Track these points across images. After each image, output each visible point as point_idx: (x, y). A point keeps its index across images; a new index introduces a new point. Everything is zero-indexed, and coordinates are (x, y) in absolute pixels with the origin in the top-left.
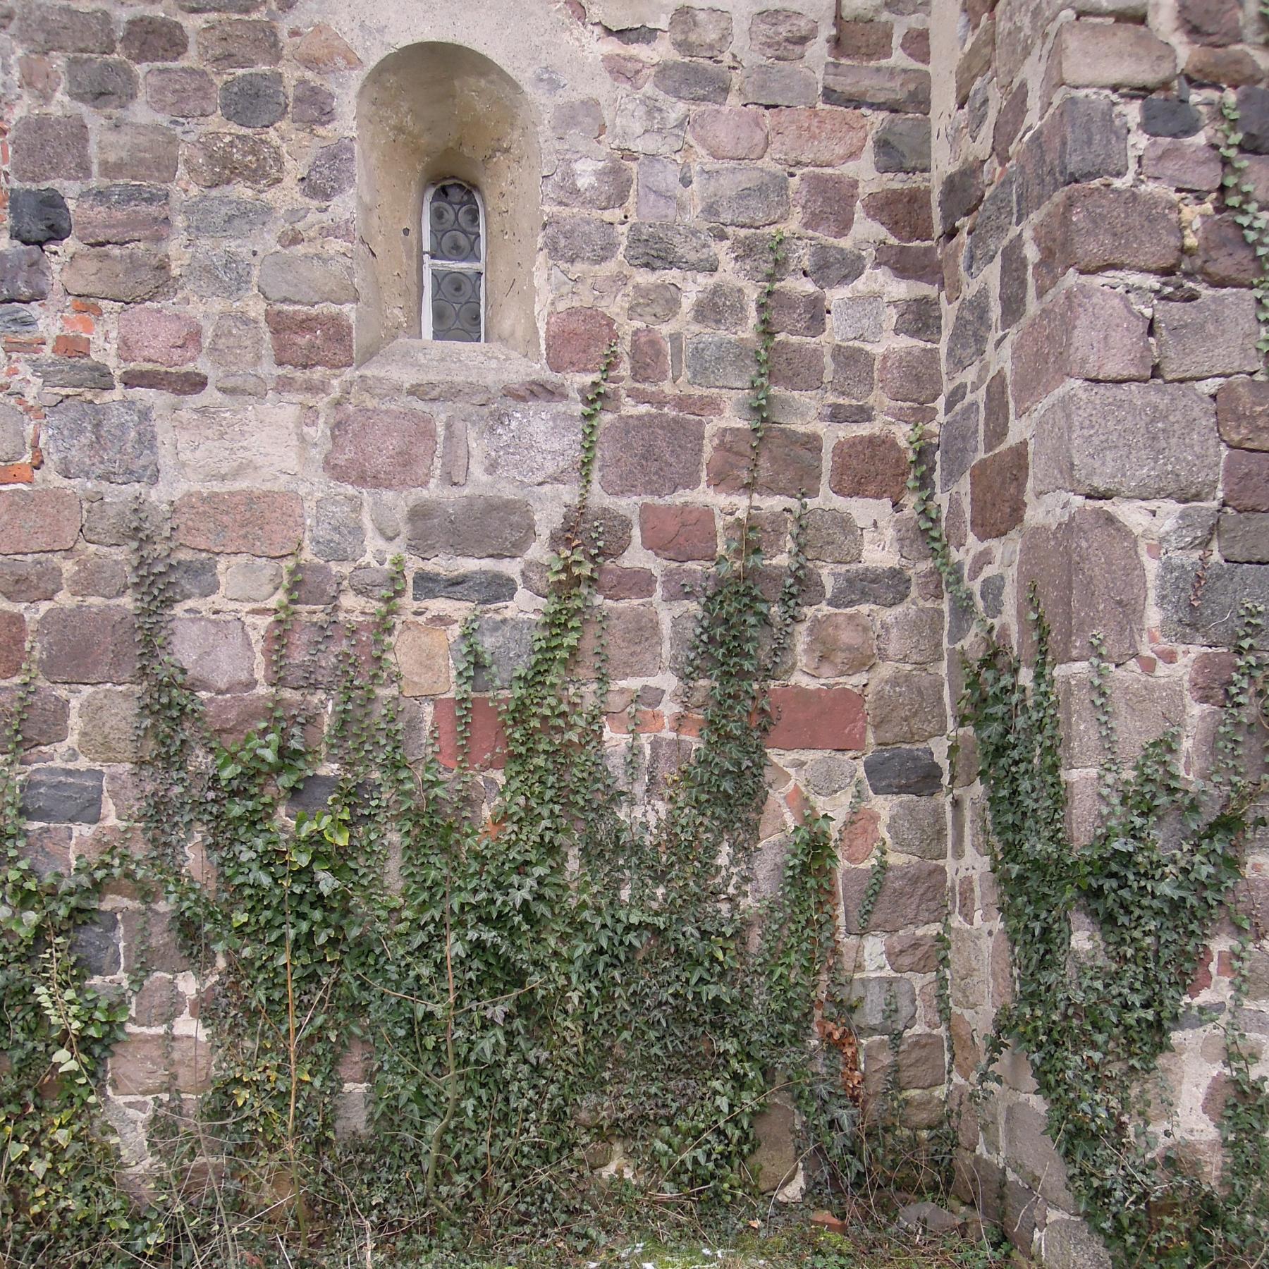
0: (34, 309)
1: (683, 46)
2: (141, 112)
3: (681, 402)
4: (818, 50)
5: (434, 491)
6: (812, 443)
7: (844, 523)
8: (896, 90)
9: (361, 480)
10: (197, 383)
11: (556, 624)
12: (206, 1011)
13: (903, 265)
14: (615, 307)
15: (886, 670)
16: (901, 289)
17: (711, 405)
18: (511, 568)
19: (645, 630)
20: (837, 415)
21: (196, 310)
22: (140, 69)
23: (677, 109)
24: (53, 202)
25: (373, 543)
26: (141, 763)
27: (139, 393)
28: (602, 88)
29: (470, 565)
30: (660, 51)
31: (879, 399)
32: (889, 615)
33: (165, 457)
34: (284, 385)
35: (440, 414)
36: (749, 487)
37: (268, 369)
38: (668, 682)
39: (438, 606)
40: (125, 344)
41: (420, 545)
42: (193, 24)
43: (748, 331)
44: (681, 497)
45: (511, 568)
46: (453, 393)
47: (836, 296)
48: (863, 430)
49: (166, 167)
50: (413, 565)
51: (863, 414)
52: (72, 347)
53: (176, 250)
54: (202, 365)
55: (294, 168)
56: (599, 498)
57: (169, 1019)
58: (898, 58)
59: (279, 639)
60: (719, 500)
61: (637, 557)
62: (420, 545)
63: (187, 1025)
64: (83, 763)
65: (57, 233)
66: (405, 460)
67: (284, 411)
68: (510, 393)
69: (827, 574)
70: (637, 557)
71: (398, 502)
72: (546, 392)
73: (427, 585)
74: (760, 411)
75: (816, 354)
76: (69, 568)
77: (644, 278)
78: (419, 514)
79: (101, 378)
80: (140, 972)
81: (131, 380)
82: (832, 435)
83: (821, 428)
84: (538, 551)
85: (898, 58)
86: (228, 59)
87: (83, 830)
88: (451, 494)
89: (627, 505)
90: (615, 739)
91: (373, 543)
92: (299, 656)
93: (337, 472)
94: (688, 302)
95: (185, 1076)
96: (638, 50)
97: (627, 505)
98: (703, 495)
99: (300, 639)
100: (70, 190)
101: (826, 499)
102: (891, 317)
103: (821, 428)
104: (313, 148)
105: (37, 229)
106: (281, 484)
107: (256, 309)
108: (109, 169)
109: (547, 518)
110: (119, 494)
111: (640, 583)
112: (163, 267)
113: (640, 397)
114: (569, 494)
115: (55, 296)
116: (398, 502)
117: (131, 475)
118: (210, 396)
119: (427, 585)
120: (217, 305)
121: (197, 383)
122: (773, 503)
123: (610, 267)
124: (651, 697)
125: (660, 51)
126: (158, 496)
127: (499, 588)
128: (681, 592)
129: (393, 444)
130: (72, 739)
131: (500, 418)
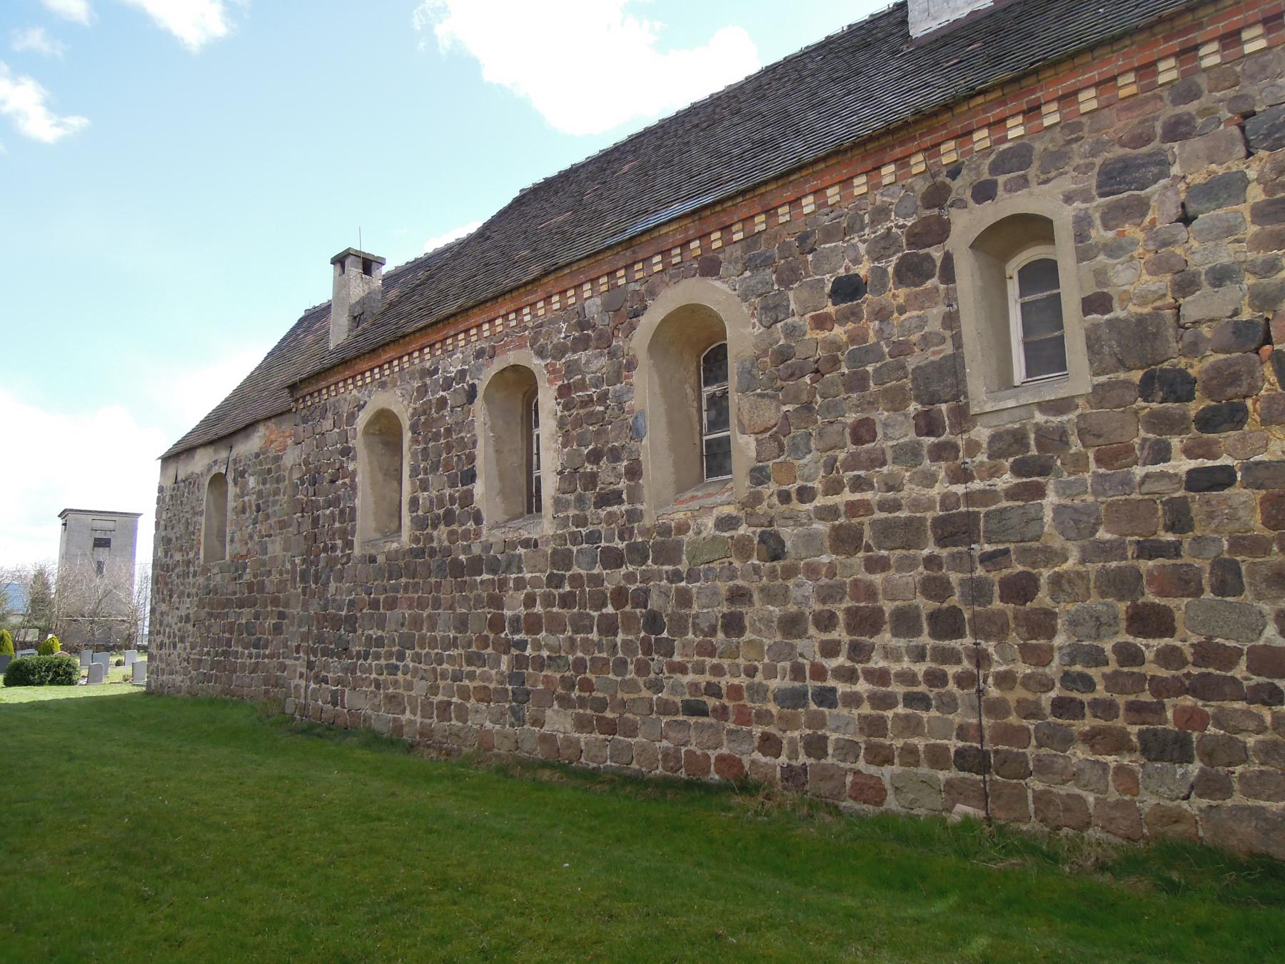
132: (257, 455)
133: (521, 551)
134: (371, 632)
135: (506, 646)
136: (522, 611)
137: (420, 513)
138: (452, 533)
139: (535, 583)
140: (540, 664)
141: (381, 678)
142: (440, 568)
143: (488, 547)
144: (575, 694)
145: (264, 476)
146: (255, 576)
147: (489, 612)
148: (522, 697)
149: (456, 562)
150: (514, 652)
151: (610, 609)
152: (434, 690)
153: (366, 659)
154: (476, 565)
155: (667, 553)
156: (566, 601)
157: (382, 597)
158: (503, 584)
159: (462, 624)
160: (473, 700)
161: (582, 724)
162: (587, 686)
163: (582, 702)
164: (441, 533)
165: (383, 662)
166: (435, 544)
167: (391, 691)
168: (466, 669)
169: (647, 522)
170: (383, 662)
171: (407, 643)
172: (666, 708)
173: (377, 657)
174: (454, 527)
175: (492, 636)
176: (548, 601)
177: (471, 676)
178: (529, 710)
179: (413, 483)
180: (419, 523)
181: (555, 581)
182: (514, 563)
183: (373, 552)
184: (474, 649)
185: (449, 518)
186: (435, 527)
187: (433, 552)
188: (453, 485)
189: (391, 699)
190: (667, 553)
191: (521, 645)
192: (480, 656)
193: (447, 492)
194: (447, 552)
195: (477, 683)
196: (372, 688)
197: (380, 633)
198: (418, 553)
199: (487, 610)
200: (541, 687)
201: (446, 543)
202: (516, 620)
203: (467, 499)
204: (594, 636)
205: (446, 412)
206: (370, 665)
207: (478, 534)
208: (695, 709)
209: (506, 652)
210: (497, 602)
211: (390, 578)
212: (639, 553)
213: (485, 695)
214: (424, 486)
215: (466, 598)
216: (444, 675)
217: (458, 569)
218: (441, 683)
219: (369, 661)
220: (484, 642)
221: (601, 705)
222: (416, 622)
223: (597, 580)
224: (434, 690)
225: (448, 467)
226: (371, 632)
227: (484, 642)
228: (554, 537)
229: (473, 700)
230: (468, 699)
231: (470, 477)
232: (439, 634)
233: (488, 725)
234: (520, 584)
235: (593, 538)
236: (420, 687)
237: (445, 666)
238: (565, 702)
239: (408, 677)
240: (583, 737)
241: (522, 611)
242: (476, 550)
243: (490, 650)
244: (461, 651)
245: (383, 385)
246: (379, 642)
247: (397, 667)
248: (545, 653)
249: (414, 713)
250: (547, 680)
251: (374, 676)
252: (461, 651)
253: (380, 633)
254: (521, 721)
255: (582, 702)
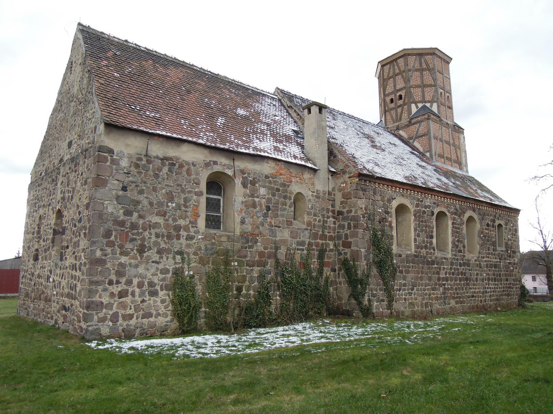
0: (267, 218)
1: (317, 193)
2: (276, 198)
3: (317, 231)
4: (327, 194)
5: (298, 239)
6: (327, 235)
7: (329, 244)
8: (332, 199)
9: (293, 238)
10: (280, 227)
11: (308, 254)
12: (280, 296)
13: (334, 217)
14: (312, 220)
15: (332, 259)
16: (333, 220)
17: (319, 231)
18: (304, 248)
19: (314, 254)
20: (328, 233)
21: (280, 219)
22: (277, 193)
23: (317, 200)
24: (269, 207)
25: (294, 245)
26: (275, 268)
27: (276, 228)
28: (311, 198)
29: (301, 247)
30: (315, 194)
31: (331, 231)
32: (332, 253)
33: (277, 235)
34: (287, 228)
35: (299, 231)
36: (322, 240)
37: (286, 226)
38: (316, 260)
39: (299, 252)
40: (275, 223)
41: (297, 245)
42: (281, 188)
43: (322, 223)
44: (317, 241)
45: (304, 248)
46: (300, 229)
47: (328, 220)
48: (330, 234)
49: (278, 204)
50: (297, 247)
51: (330, 233)
52: (270, 222)
53: (279, 213)
54: (281, 225)
55: (288, 205)
56: (311, 241)
57: (276, 297)
58: (333, 196)
59: (286, 255)
60: (320, 241)
61: (314, 247)
62: (297, 245)
63: (278, 298)
64: (270, 268)
65: (270, 210)
66: (296, 236)
67: (287, 230)
68: (304, 229)
69: (328, 249)
70: (314, 247)
71: (295, 240)
72: (307, 229)
73: (298, 249)
74: (323, 232)
75: (327, 226)
76: (269, 246)
77: (314, 218)
78: (297, 242)
79: (272, 226)
80: (274, 292)
81: (275, 226)
82: (328, 234)
83: (327, 234)
84: (306, 246)
85: (333, 196)
86: (283, 193)
87: (270, 276)
88: (300, 240)
89: (313, 241)
90: (312, 266)
91: (294, 245)
92: (288, 257)
93: (291, 237)
94: (317, 220)
95: (278, 303)
96: (313, 194)
97: (313, 241)
98: (319, 241)
99: (288, 255)
100: (271, 205)
101: (328, 241)
102: (332, 223)
103: (327, 234)
104: (290, 202)
105: (268, 210)
106: (287, 238)
107: (285, 219)
108: (274, 204)
109: (307, 243)
110: (274, 238)
111: (314, 250)
112: (278, 214)
113: (314, 230)
114: (308, 240)
115: (269, 217)
116: (295, 240)
117: (275, 237)
118: (281, 228)
119: (298, 249)
120: (282, 219)
121: (280, 227)
122: (324, 242)
123: (312, 216)
124: (315, 262)
125: (315, 194)
126: (277, 239)
127: (303, 250)
128: (317, 251)
129: (295, 234)
130: (269, 265)
131: (304, 232)
132: (267, 177)
133: (444, 260)
134: (401, 281)
135: (440, 285)
136: (444, 276)
137: (417, 243)
138: (427, 252)
139: (447, 269)
140: (448, 289)
141: (406, 297)
142: (424, 262)
143: (436, 258)
144: (456, 295)
145: (274, 191)
146: (265, 248)
147: (437, 276)
148: (445, 298)
149: (428, 261)
150: (443, 287)
151: (460, 276)
152: (423, 299)
153: (399, 291)
154: (433, 263)
155: (468, 265)
156: (453, 274)
157: (404, 269)
158: (440, 268)
159: (430, 279)
160: (434, 301)
161: (457, 303)
162: (457, 294)
163: (457, 298)
164: (424, 251)
165: (406, 292)
166: (422, 254)
167: (410, 301)
168: (432, 292)
169: (466, 258)
170: (406, 292)
171: (414, 285)
172: (469, 297)
173: (404, 290)
174: (428, 250)
175: (438, 282)
176: (450, 274)
177: (434, 294)
178: (447, 301)
179: (415, 233)
180: (417, 247)
181: (451, 269)
182: (442, 263)
183: (401, 253)
184: (433, 286)
185: (426, 247)
186: (422, 249)
187: (421, 257)
188: (427, 238)
189: (411, 304)
190: (468, 265)
191: (444, 285)
192: (435, 288)
193: (426, 239)
194: (425, 257)
195: (435, 296)
196: (404, 301)
197: (404, 282)
198: (416, 256)
199: (436, 275)
200: (449, 295)
201: (425, 255)
202: (443, 278)
203: (431, 243)
204: (458, 282)
205: (425, 215)
206: (402, 293)
207: (434, 254)
208: (473, 296)
209: (442, 287)
210: (438, 273)
211: (407, 263)
212: (464, 264)
213: (437, 299)
214: (418, 236)
215: (431, 272)
216: (426, 294)
217: (428, 263)
218: (425, 297)
219: (401, 292)
220: (436, 284)
221: (460, 298)
222: (416, 278)
223: (458, 269)
224: (423, 299)
225: (426, 232)
226: (401, 281)
227: (436, 284)
228: (451, 258)
229: (434, 301)
230: (433, 301)
231: (432, 237)
232: (424, 282)
233: (438, 307)
234: (444, 269)
235: (457, 260)
236: (420, 298)
237: (426, 291)
238: (454, 298)
239: (416, 296)
240: (457, 306)
241: (444, 276)
242: (433, 258)
243: (437, 286)
244: (430, 287)
245: (403, 196)
246: (405, 285)
247: (412, 293)
248: (450, 287)
249: (418, 307)
250: (451, 293)
251: (404, 297)
252: (430, 287)
253: (404, 282)
254: (445, 304)
255: (457, 298)
